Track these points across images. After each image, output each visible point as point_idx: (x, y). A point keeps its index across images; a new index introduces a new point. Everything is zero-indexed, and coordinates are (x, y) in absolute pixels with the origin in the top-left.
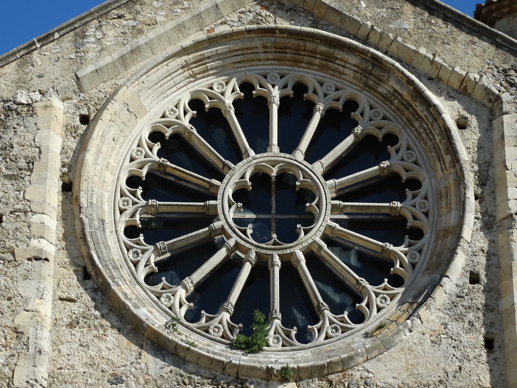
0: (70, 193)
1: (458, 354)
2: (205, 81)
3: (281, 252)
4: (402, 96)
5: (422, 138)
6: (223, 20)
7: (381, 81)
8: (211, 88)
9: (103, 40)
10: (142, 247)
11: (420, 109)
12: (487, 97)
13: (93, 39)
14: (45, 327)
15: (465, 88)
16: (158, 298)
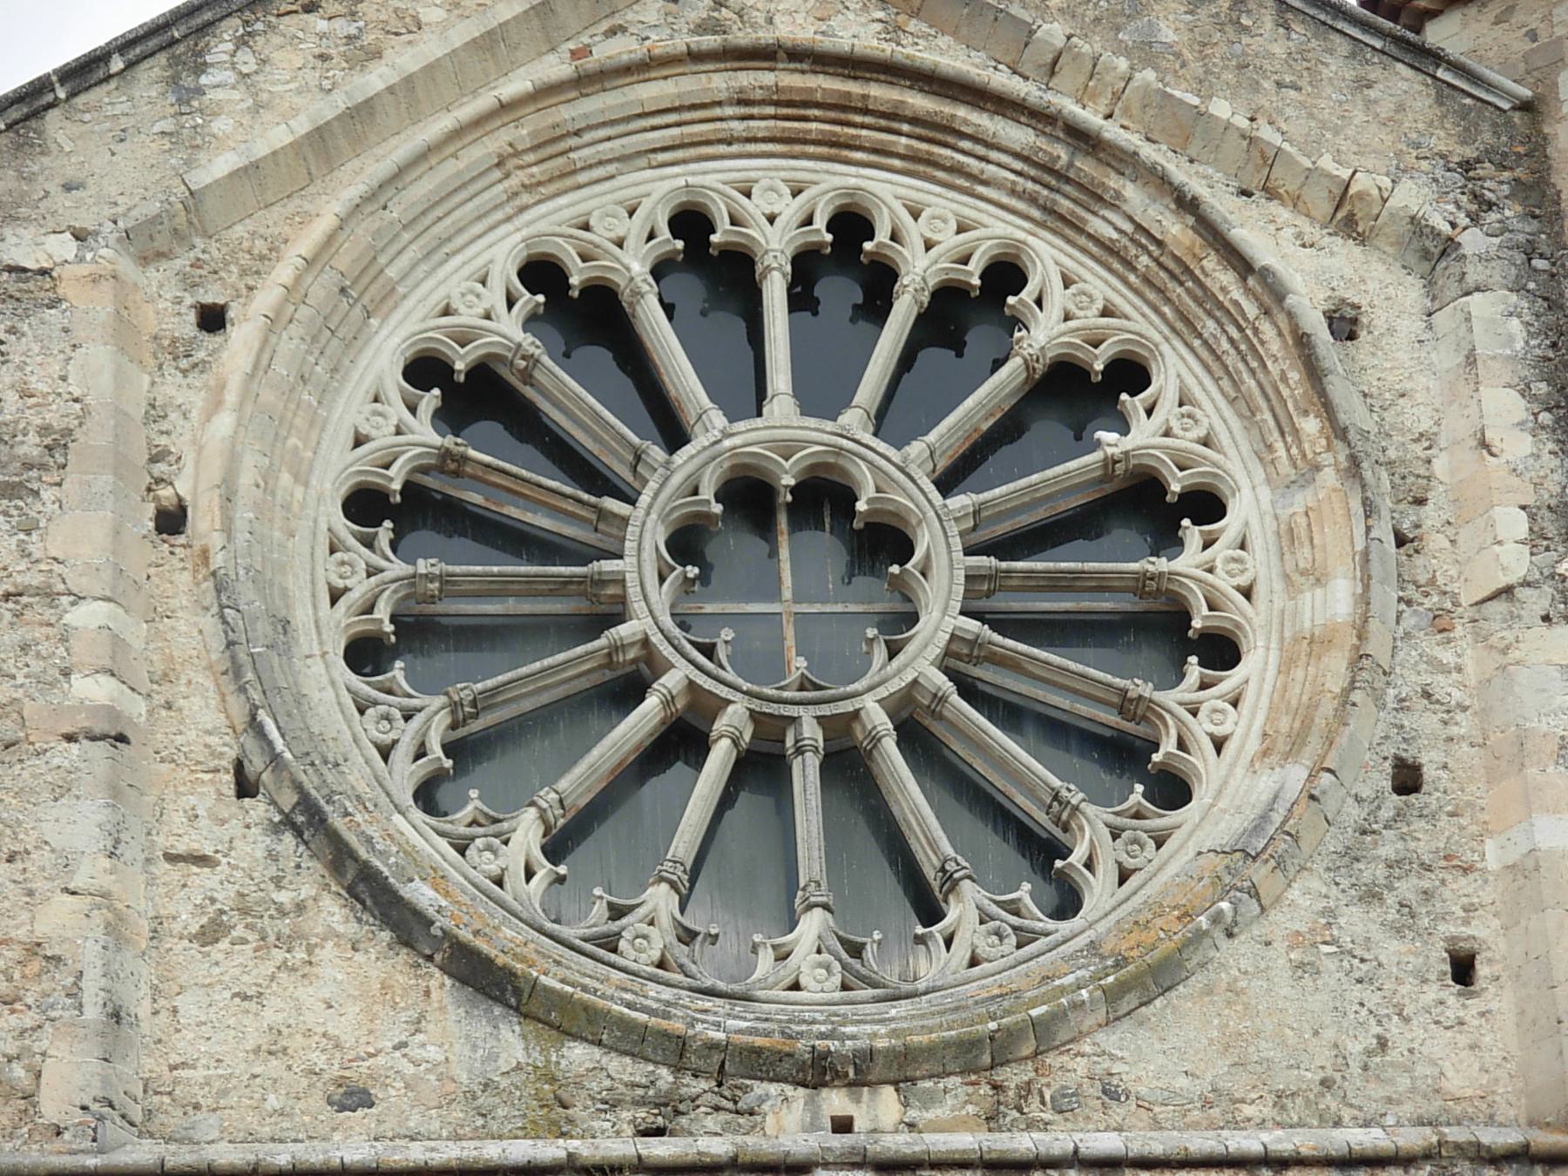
0: (181, 539)
1: (1373, 999)
2: (568, 206)
3: (826, 710)
6: (617, 20)
8: (586, 227)
9: (260, 78)
10: (405, 701)
12: (1415, 244)
13: (229, 76)
14: (128, 941)
15: (1350, 221)
16: (462, 851)
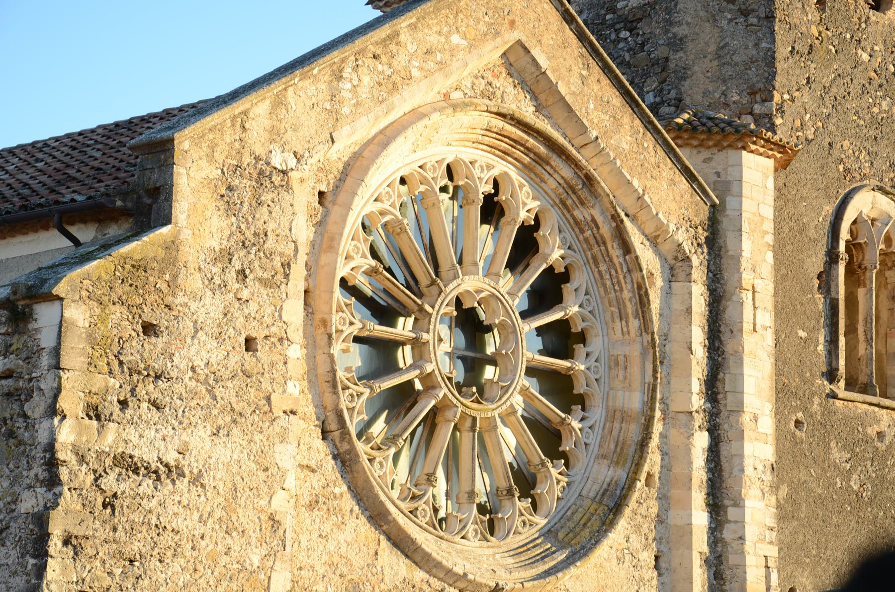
4: (598, 228)
5: (604, 285)
7: (582, 203)
11: (616, 252)
12: (675, 254)
